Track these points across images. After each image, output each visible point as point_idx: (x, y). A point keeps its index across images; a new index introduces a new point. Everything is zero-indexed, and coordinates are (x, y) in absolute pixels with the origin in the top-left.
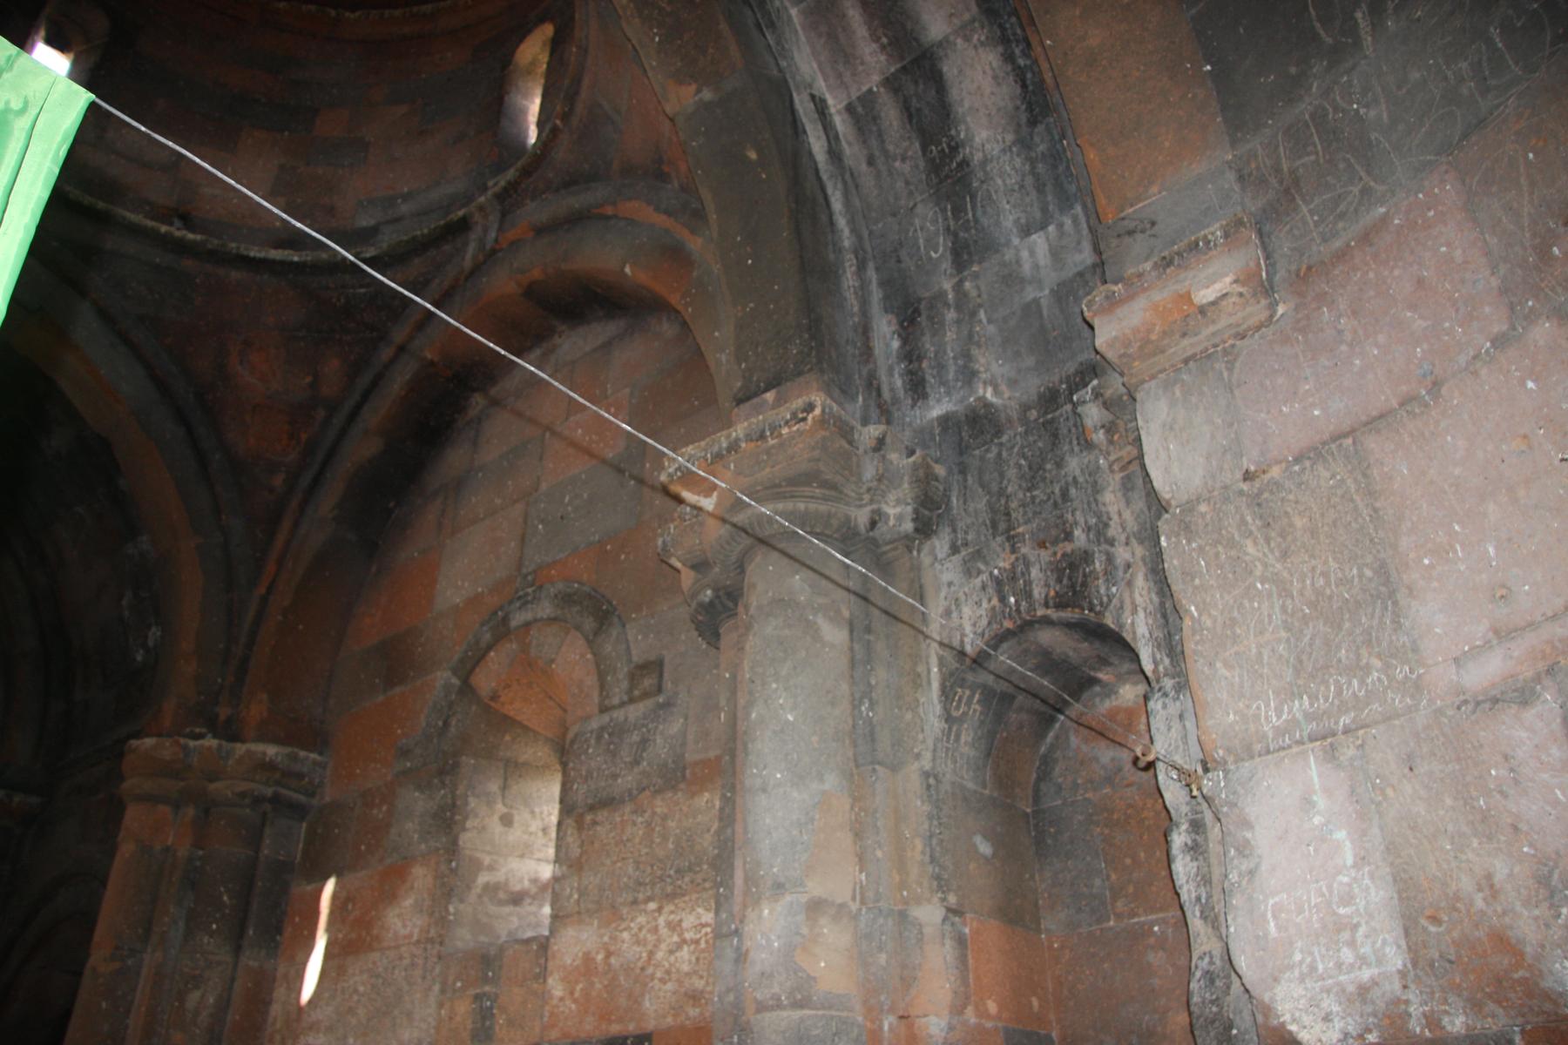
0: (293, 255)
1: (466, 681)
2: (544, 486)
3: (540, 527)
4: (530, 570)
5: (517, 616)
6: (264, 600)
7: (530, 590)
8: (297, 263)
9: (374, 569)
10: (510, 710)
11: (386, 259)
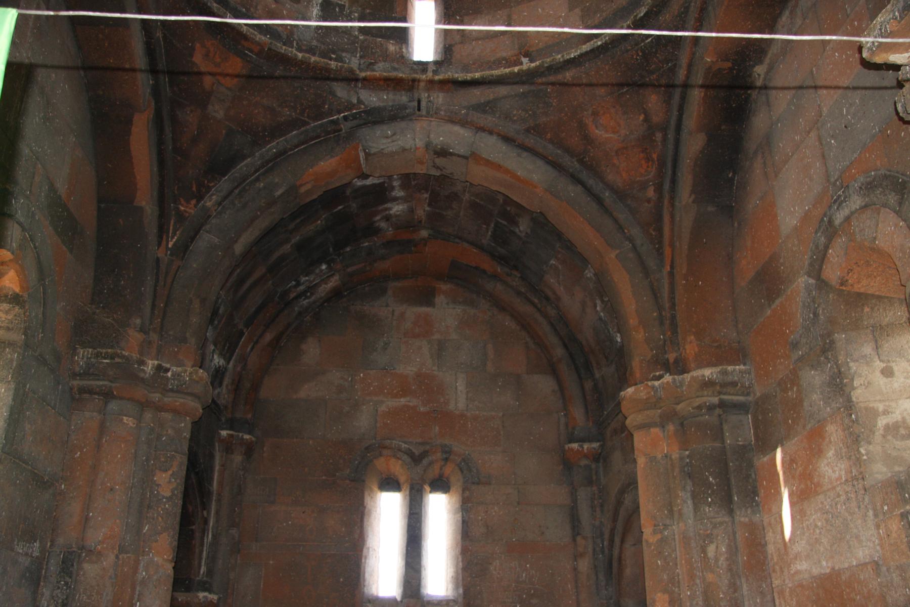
0: (596, 42)
1: (818, 278)
2: (825, 111)
3: (833, 141)
4: (836, 177)
5: (838, 216)
6: (671, 274)
7: (840, 193)
8: (601, 45)
9: (736, 225)
10: (860, 288)
11: (655, 9)
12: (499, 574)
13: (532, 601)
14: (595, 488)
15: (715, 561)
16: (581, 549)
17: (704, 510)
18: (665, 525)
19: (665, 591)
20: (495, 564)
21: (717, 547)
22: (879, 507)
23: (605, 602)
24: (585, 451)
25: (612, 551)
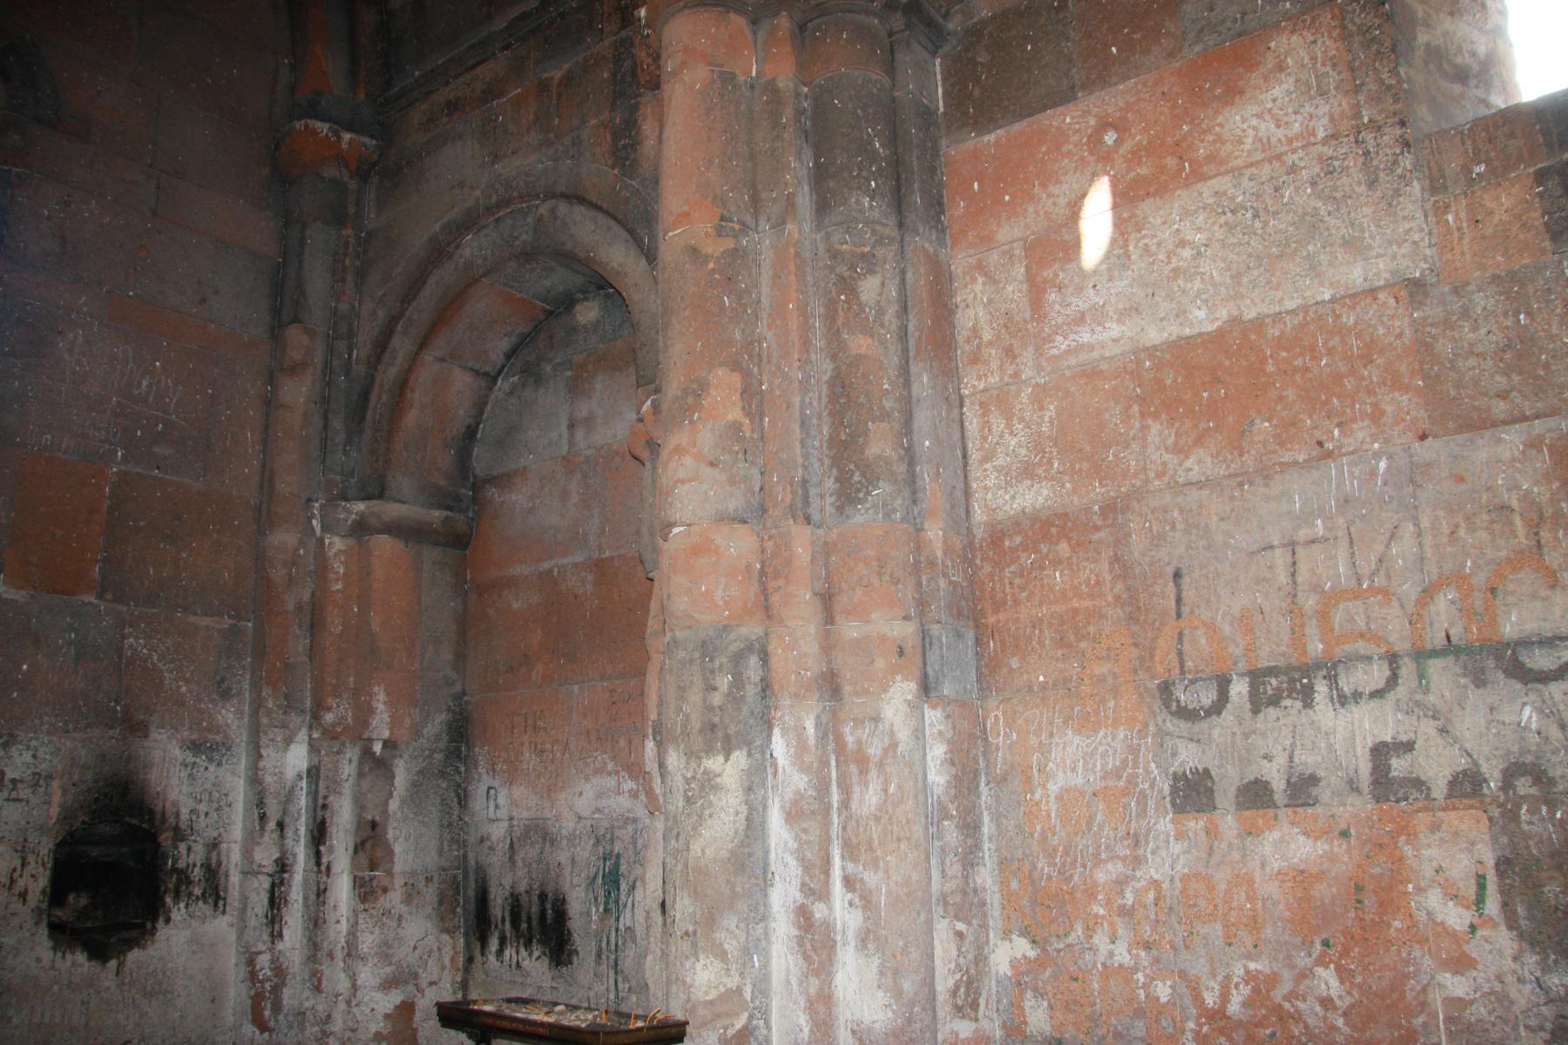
12: (79, 363)
13: (155, 449)
14: (349, 232)
15: (877, 312)
16: (296, 355)
17: (858, 202)
18: (743, 224)
19: (735, 366)
20: (71, 336)
21: (883, 284)
22: (1453, 166)
23: (338, 478)
24: (345, 146)
25: (376, 370)
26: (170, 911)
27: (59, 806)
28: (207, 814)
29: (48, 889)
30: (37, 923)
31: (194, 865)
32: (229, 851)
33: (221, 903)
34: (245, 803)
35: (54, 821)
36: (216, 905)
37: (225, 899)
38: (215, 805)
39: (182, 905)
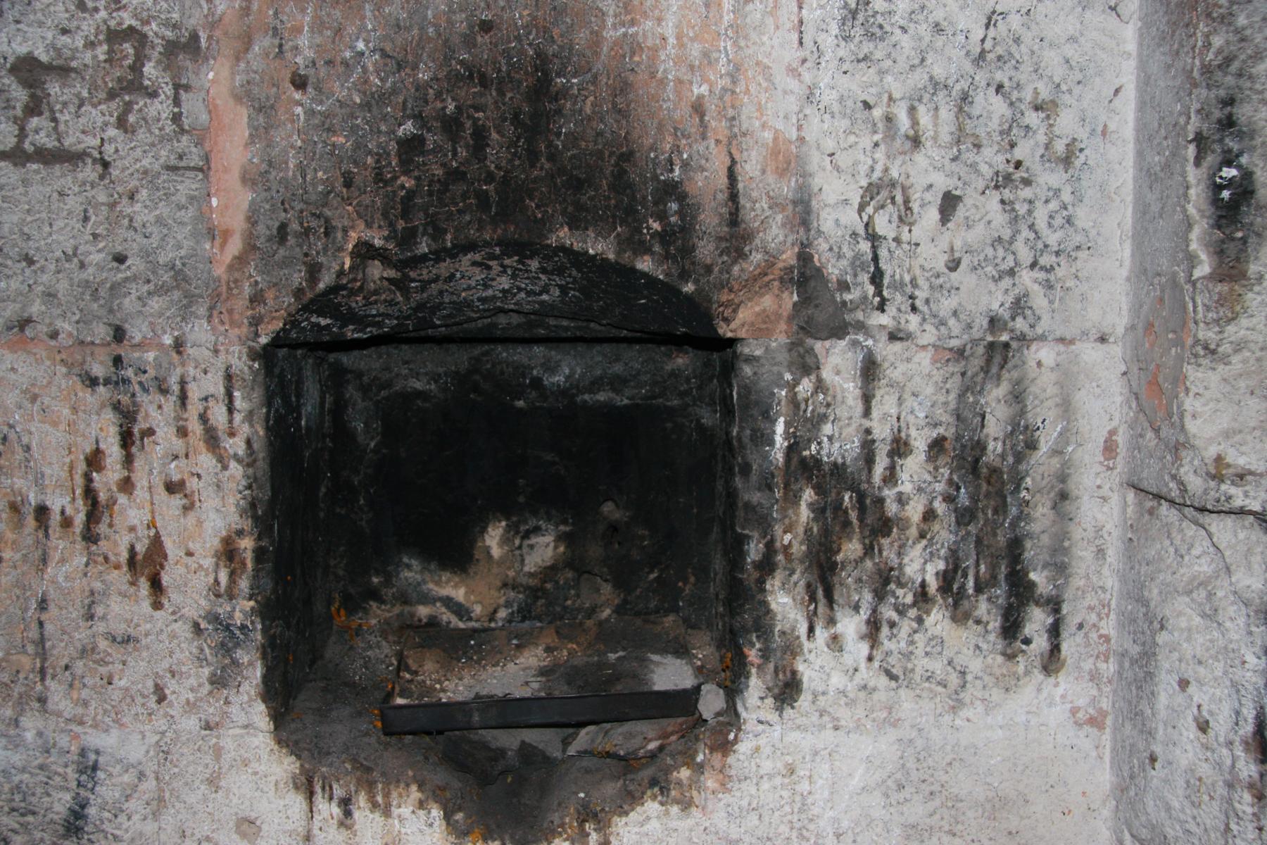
26: (792, 649)
27: (248, 180)
28: (949, 204)
29: (247, 544)
30: (218, 682)
31: (900, 448)
32: (1067, 379)
33: (1036, 621)
34: (1144, 136)
35: (235, 246)
36: (1011, 628)
37: (1054, 605)
38: (992, 159)
39: (850, 625)
